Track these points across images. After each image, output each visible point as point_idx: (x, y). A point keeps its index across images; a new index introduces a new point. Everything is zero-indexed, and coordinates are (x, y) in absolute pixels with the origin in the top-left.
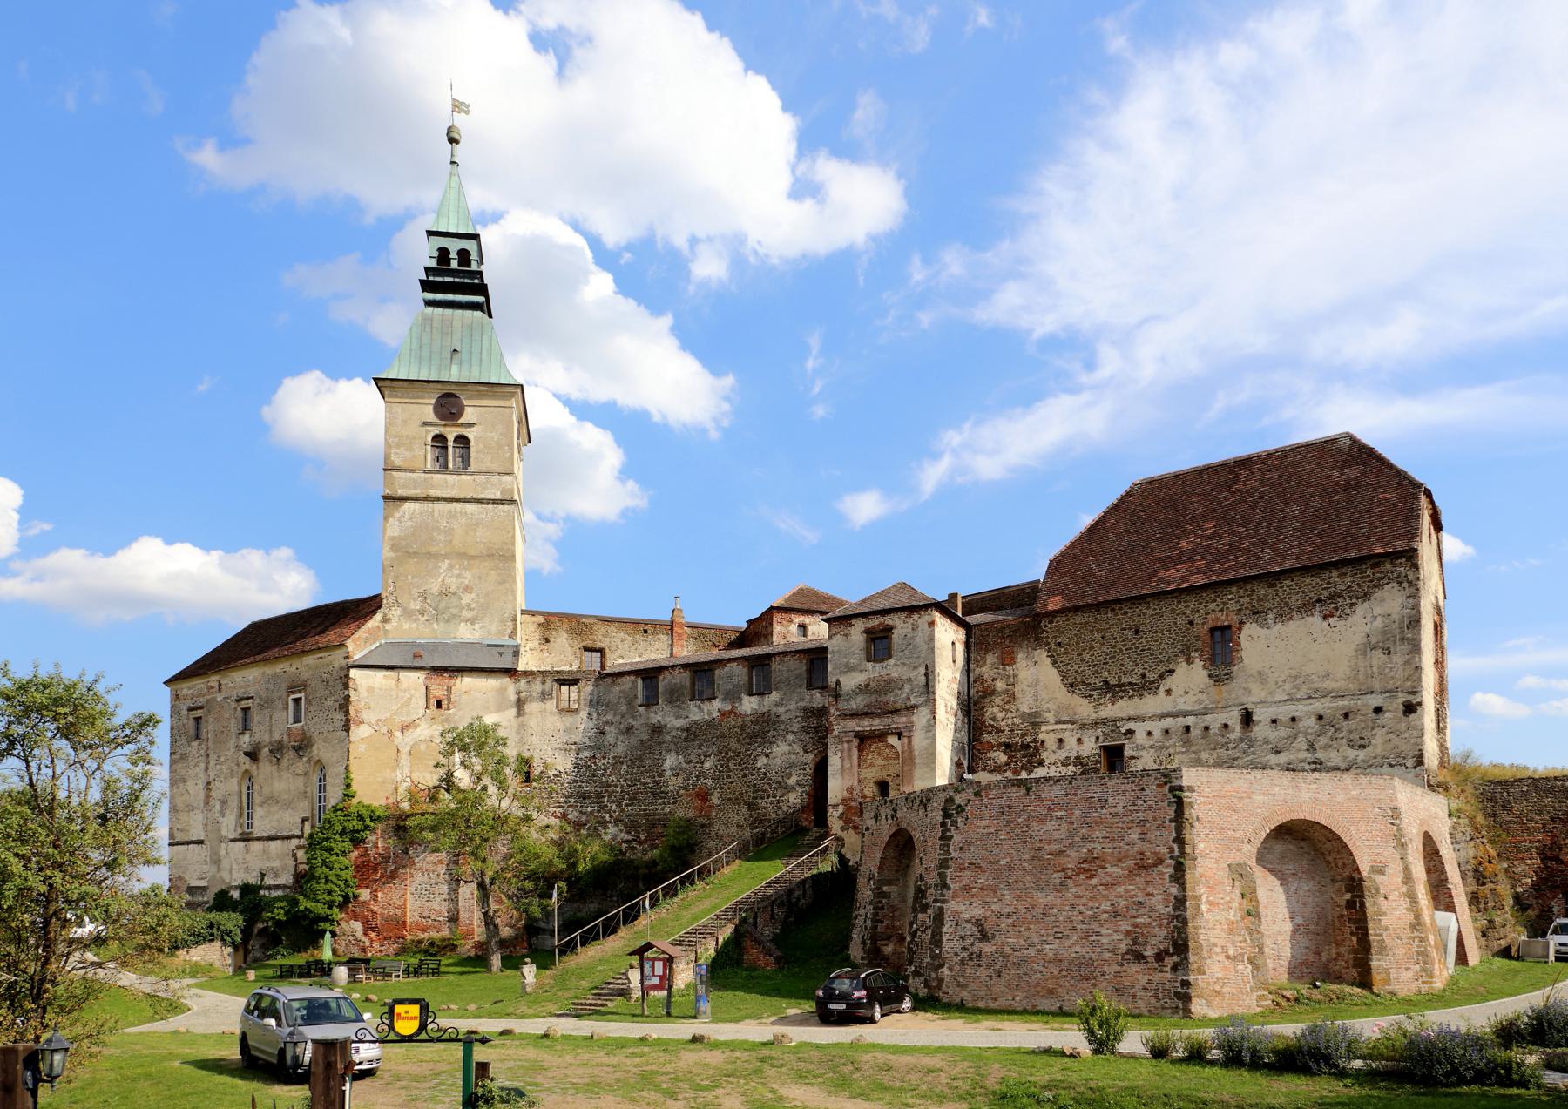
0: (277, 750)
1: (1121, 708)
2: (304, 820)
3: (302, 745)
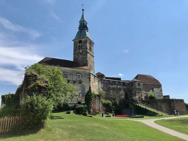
0: (74, 82)
1: (147, 92)
2: (80, 93)
3: (80, 82)
